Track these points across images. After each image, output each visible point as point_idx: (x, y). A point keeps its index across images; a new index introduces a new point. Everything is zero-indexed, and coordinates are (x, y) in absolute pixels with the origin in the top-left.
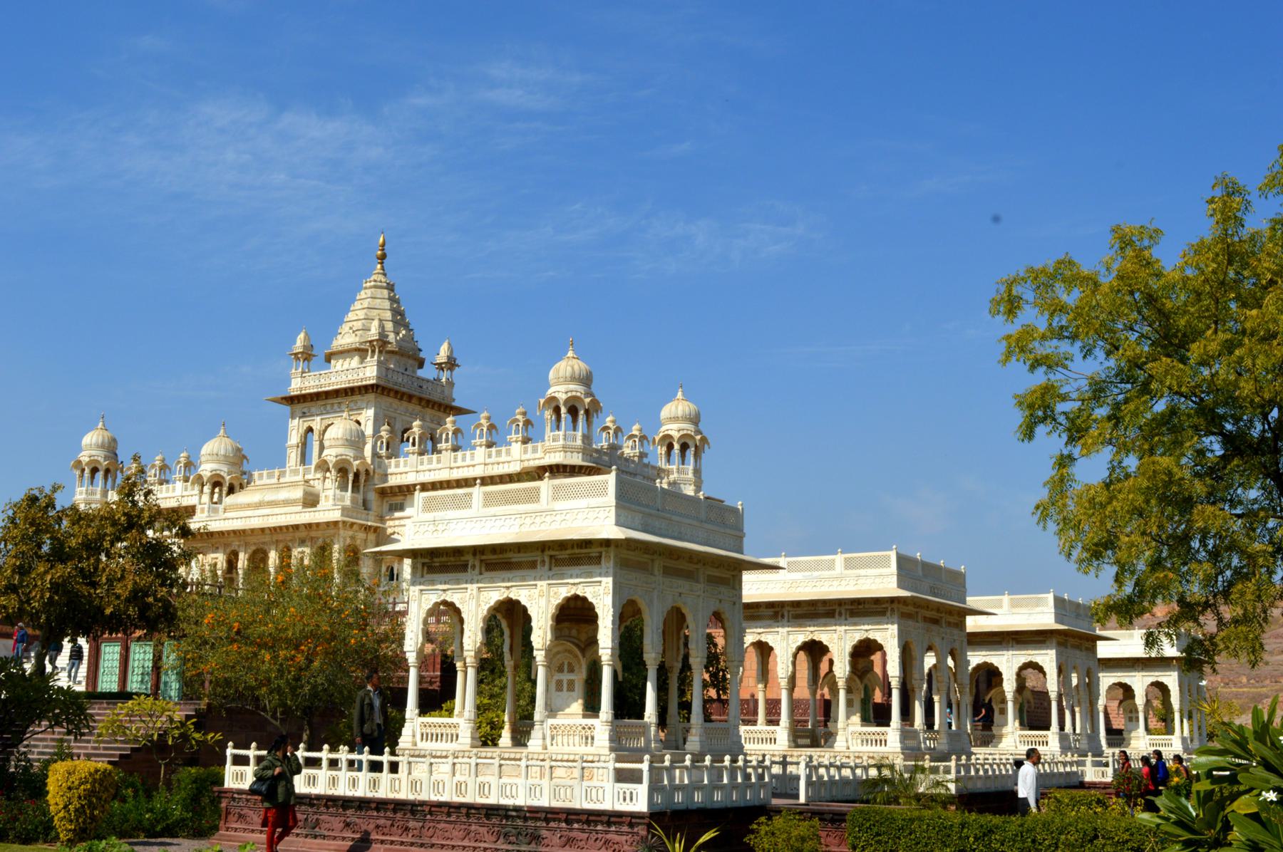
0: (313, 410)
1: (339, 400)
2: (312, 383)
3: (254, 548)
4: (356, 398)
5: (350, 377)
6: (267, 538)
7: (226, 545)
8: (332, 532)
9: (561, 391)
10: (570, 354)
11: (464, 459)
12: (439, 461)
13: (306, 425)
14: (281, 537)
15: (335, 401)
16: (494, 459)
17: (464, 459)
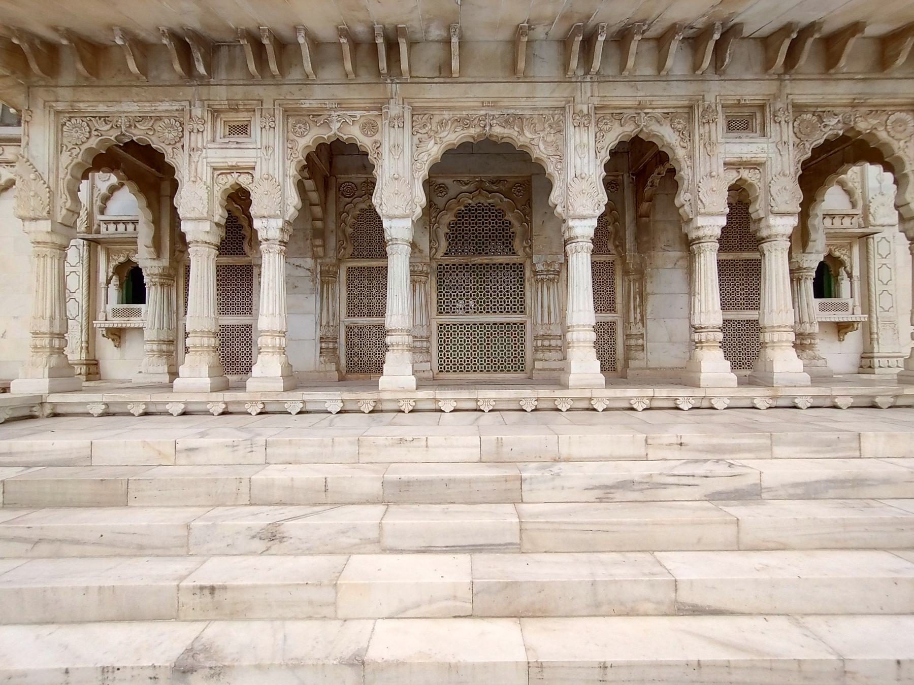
3: (453, 137)
14: (621, 95)
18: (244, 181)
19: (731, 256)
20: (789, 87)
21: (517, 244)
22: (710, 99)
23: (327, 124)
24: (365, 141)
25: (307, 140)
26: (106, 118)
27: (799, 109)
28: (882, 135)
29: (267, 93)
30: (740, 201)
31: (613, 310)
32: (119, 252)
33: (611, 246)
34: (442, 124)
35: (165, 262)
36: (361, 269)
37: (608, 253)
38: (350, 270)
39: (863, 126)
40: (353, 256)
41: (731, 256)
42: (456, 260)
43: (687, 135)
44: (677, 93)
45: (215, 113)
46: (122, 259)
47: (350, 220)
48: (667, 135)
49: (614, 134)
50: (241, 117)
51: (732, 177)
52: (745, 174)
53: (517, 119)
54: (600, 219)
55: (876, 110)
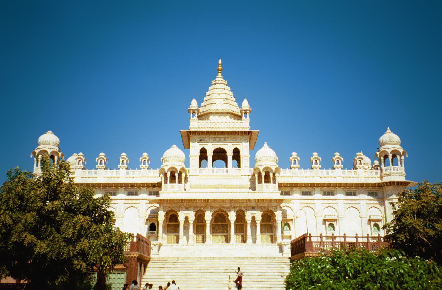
0: (207, 139)
1: (226, 136)
2: (204, 126)
3: (215, 209)
4: (237, 136)
5: (231, 126)
6: (228, 205)
7: (195, 207)
8: (275, 204)
9: (389, 148)
10: (389, 131)
11: (327, 173)
12: (311, 173)
13: (201, 147)
15: (223, 136)
16: (347, 175)
17: (327, 173)
18: (187, 215)
19: (263, 223)
20: (259, 204)
21: (227, 221)
22: (249, 205)
23: (199, 208)
24: (204, 210)
25: (196, 210)
26: (169, 207)
27: (261, 207)
28: (272, 210)
29: (191, 204)
30: (253, 218)
31: (243, 233)
32: (151, 221)
33: (243, 221)
34: (214, 208)
35: (165, 224)
36: (199, 225)
37: (243, 222)
38: (197, 225)
39: (270, 209)
40: (197, 223)
41: (263, 223)
42: (216, 223)
43: (246, 209)
44: (245, 205)
45: (184, 206)
46: (152, 222)
47: (197, 216)
48: (244, 209)
49: (237, 209)
50: (187, 207)
51: (252, 215)
52: (254, 215)
53: (223, 207)
54: (235, 221)
55: (271, 207)
